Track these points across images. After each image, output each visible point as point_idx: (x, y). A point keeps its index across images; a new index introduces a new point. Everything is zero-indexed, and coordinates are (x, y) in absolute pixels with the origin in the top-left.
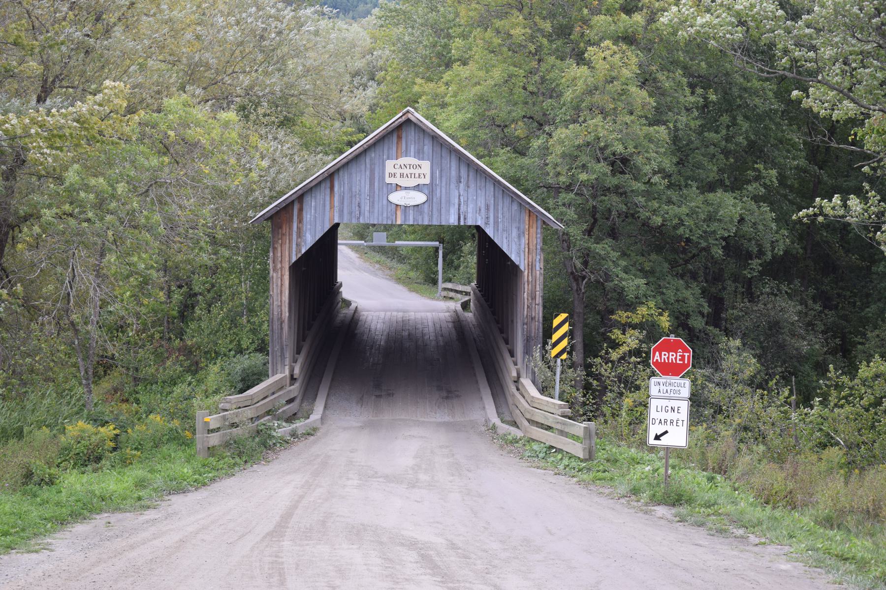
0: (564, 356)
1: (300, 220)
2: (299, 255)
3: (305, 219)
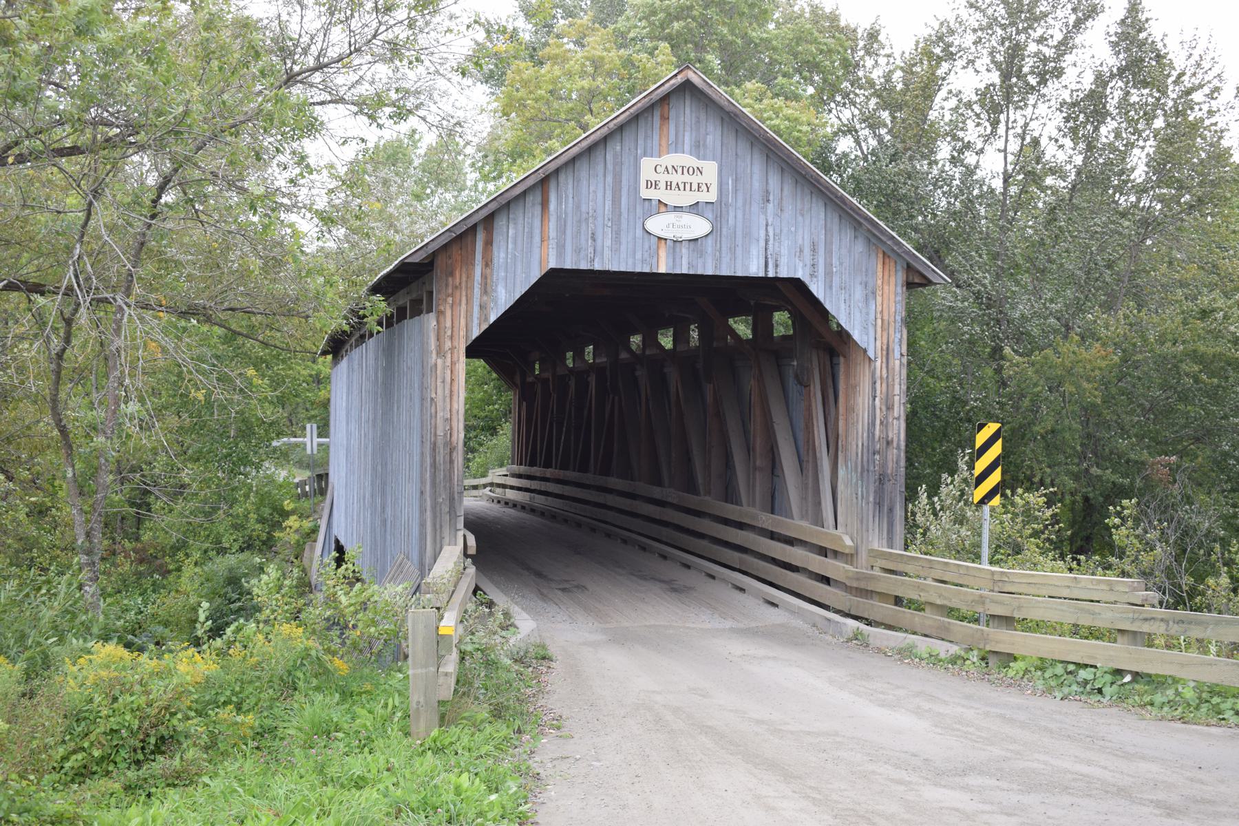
0: (996, 501)
1: (488, 263)
2: (485, 327)
3: (495, 261)
